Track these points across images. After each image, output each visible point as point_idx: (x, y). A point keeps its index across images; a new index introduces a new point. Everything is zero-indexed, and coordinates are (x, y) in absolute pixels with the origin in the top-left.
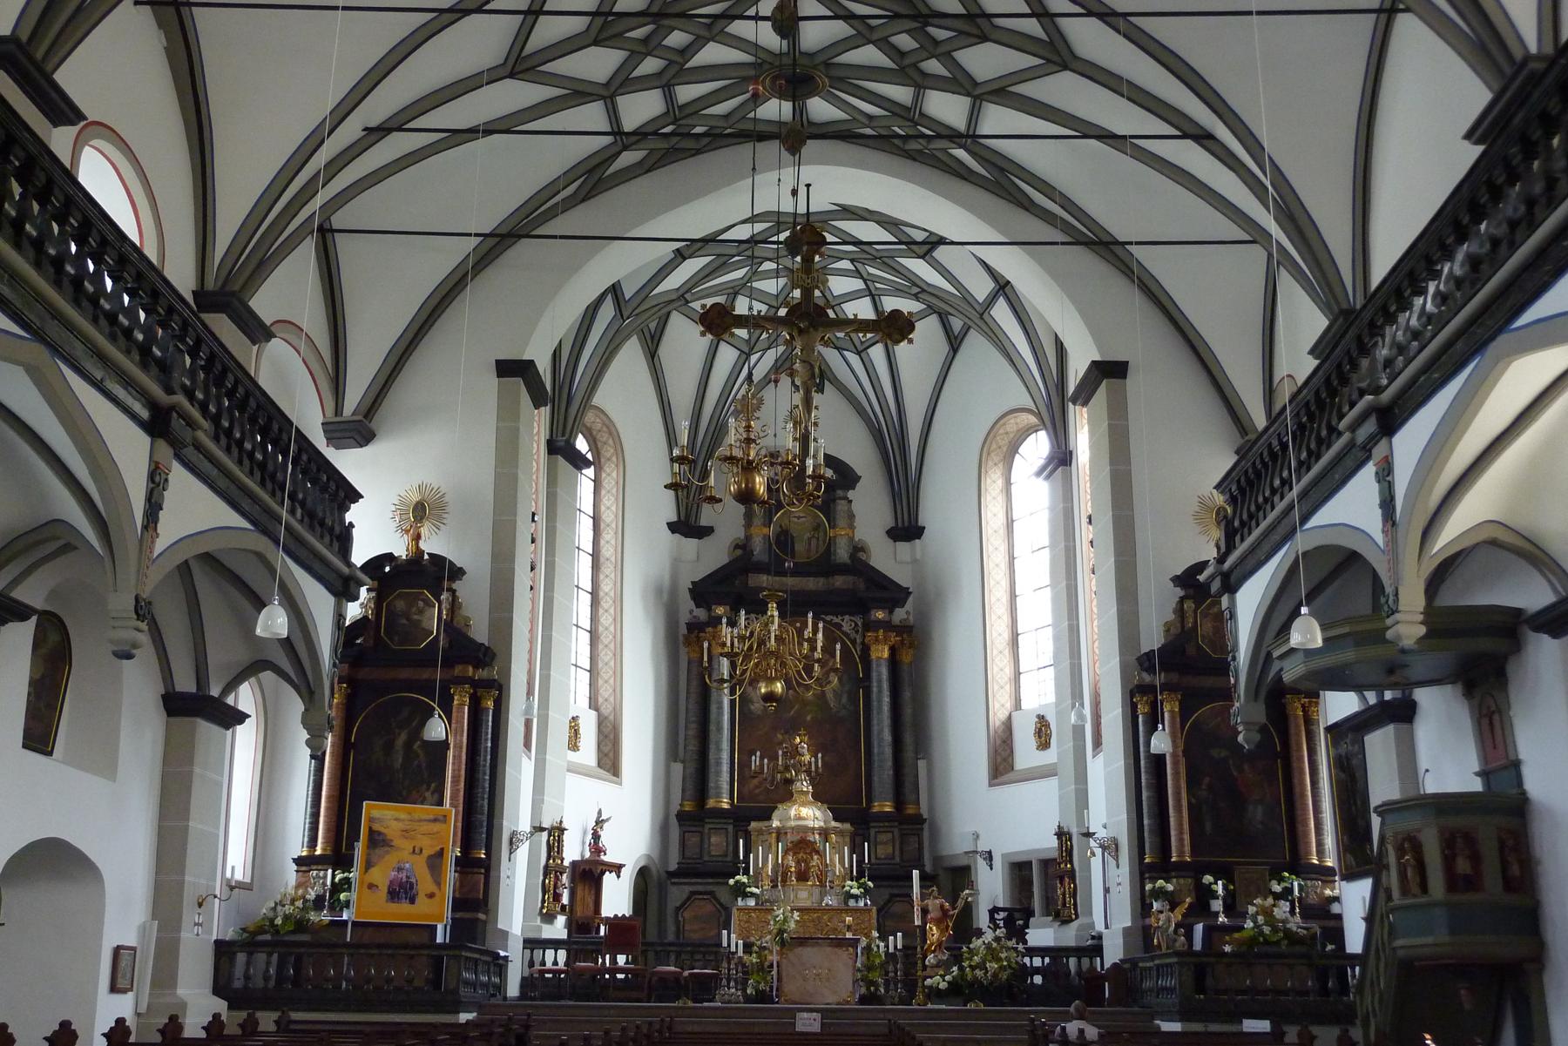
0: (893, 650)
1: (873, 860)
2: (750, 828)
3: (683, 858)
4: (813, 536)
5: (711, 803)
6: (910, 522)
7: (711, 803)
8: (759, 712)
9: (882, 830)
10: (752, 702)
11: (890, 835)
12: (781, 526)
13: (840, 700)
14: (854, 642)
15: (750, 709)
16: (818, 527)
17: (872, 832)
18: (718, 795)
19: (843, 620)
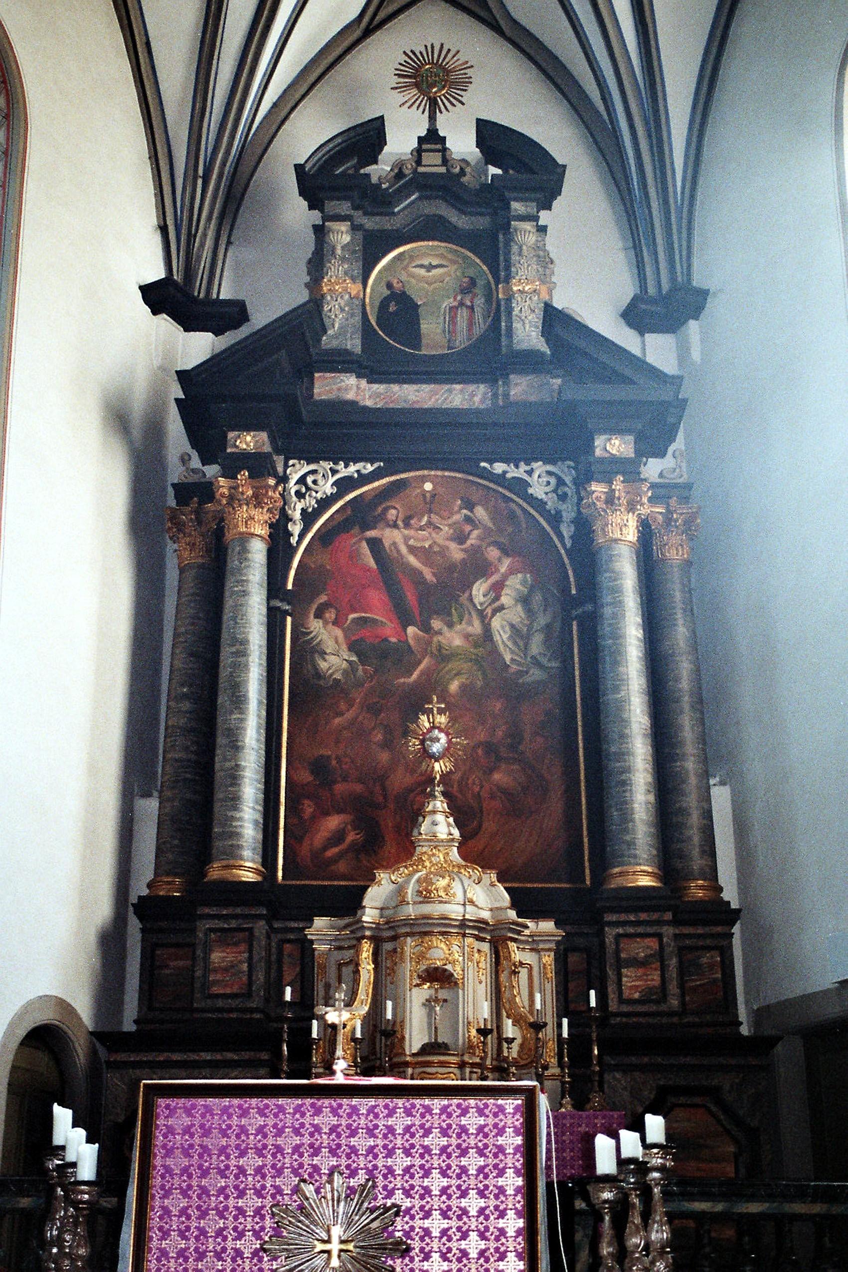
0: (646, 529)
1: (613, 1006)
2: (310, 933)
3: (150, 1008)
4: (461, 304)
5: (215, 872)
6: (673, 279)
7: (215, 872)
8: (338, 676)
9: (631, 930)
10: (323, 654)
11: (653, 943)
12: (389, 286)
13: (526, 646)
14: (555, 519)
15: (315, 667)
16: (468, 288)
17: (610, 933)
18: (233, 852)
19: (530, 473)
